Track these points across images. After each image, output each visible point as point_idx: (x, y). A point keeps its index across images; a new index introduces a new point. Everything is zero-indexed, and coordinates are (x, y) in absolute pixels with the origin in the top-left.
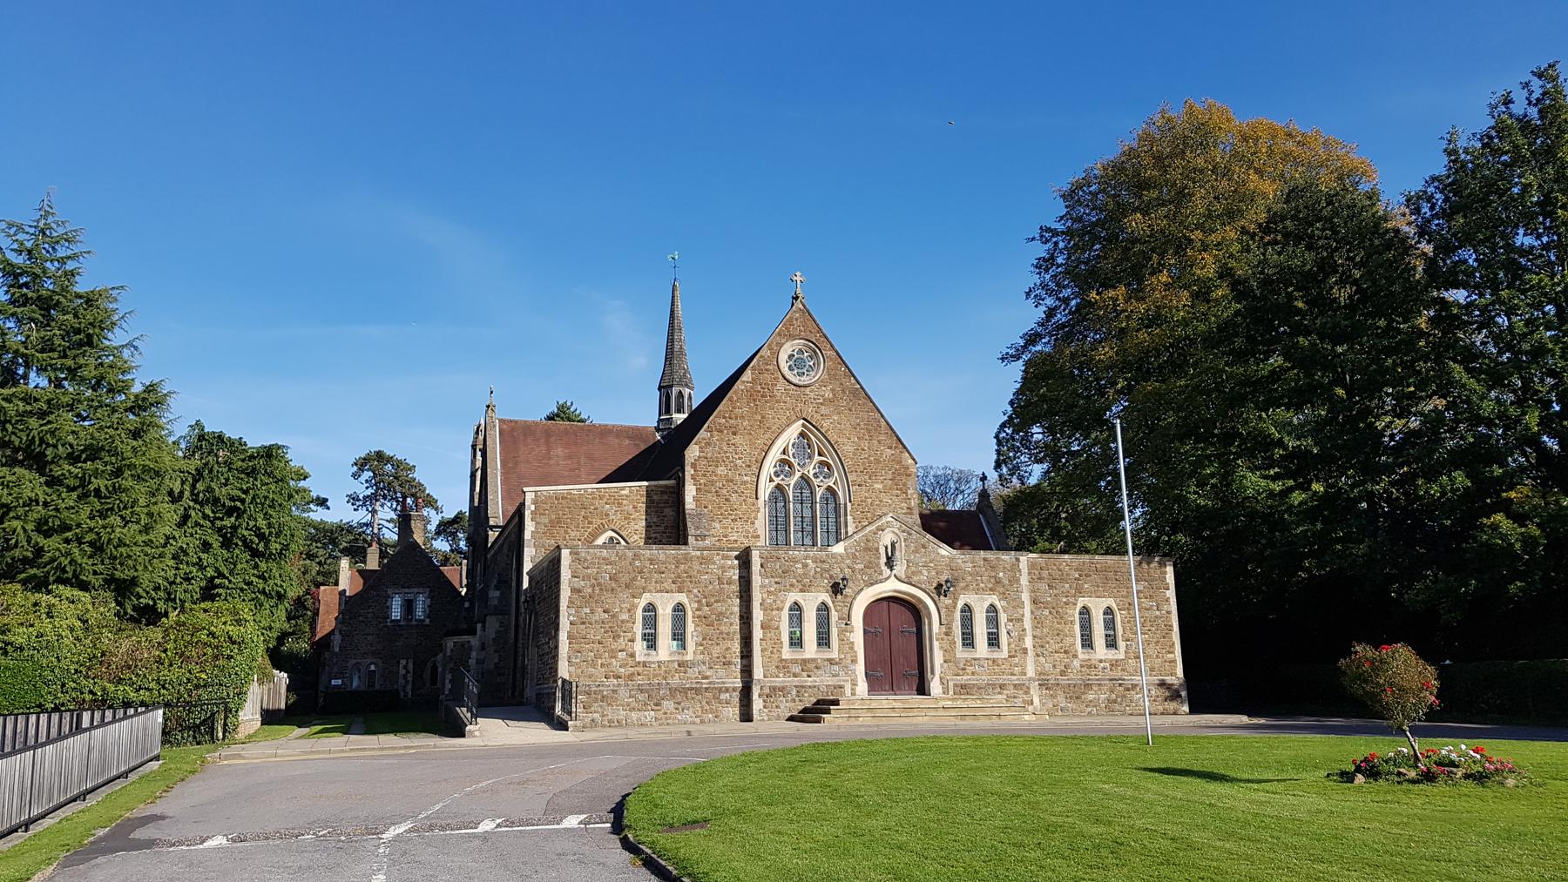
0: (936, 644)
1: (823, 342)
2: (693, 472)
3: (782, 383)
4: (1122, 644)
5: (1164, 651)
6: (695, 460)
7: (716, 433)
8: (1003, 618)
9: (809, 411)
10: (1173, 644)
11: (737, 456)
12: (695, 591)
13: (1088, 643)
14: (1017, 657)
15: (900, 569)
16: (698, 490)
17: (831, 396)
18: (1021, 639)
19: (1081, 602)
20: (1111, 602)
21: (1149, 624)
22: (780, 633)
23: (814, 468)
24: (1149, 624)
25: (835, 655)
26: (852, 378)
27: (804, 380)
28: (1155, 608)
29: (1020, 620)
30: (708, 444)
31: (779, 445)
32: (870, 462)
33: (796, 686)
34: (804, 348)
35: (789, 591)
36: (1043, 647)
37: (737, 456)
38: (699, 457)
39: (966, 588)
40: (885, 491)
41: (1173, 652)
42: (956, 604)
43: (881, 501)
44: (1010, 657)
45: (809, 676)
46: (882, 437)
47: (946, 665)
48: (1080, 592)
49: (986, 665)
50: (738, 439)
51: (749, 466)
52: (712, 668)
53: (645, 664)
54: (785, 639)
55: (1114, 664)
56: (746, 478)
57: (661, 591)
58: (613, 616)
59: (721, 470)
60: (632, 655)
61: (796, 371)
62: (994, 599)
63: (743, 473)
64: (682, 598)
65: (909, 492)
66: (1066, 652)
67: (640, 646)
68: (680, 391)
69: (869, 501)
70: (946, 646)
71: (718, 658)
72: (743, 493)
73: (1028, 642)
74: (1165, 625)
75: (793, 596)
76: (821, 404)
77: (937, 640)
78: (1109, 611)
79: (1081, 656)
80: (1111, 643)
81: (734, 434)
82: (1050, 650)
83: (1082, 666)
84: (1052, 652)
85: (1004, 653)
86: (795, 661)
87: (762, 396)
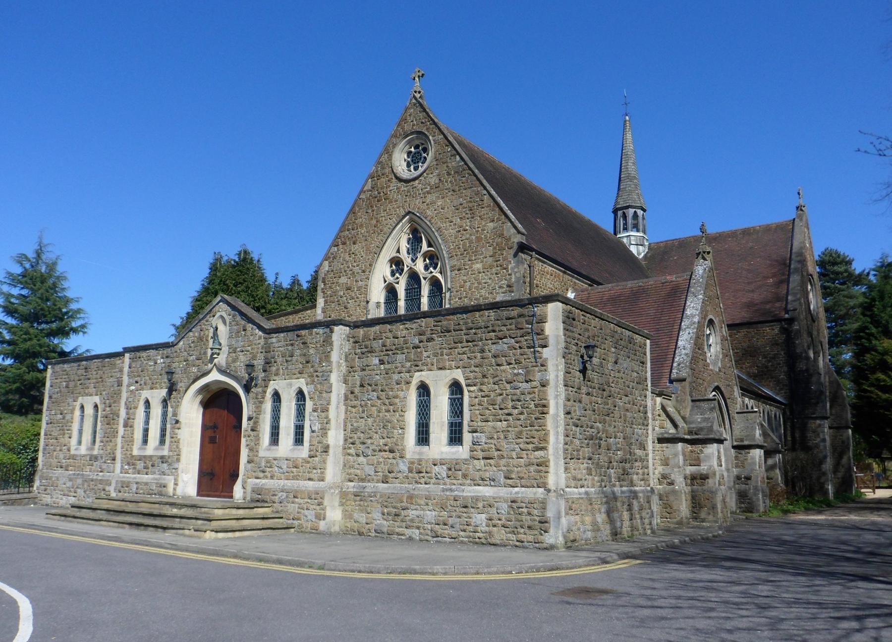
0: (243, 440)
1: (433, 128)
2: (323, 286)
3: (394, 183)
4: (467, 437)
5: (530, 446)
6: (325, 275)
7: (341, 246)
8: (309, 405)
9: (416, 205)
10: (547, 435)
11: (355, 264)
12: (104, 393)
13: (423, 437)
14: (316, 456)
15: (222, 359)
16: (326, 302)
17: (437, 181)
18: (324, 431)
19: (417, 377)
20: (459, 375)
21: (510, 404)
22: (133, 430)
23: (425, 260)
24: (510, 404)
25: (165, 452)
26: (457, 157)
27: (421, 170)
28: (521, 378)
29: (325, 410)
30: (334, 258)
31: (390, 244)
32: (471, 242)
33: (137, 483)
34: (417, 142)
35: (142, 389)
36: (364, 443)
37: (355, 264)
38: (328, 272)
39: (277, 374)
40: (487, 268)
41: (543, 449)
42: (265, 392)
43: (479, 283)
44: (311, 457)
45: (147, 474)
46: (484, 211)
47: (249, 466)
48: (417, 366)
49: (284, 467)
50: (354, 248)
51: (364, 272)
52: (105, 462)
53: (74, 457)
54: (138, 435)
55: (453, 467)
56: (360, 283)
57: (87, 395)
58: (64, 418)
59: (343, 280)
60: (69, 450)
61: (420, 164)
62: (301, 383)
63: (359, 279)
64: (97, 399)
65: (510, 267)
66: (392, 451)
67: (74, 441)
68: (635, 212)
69: (468, 284)
70: (252, 444)
71: (110, 454)
72: (357, 298)
73: (335, 437)
74: (536, 406)
75: (146, 394)
76: (428, 193)
77: (245, 436)
78: (456, 388)
79: (408, 456)
80: (455, 437)
81: (354, 243)
82: (374, 447)
83: (410, 471)
84: (374, 451)
85: (304, 452)
86: (141, 458)
87: (378, 201)
